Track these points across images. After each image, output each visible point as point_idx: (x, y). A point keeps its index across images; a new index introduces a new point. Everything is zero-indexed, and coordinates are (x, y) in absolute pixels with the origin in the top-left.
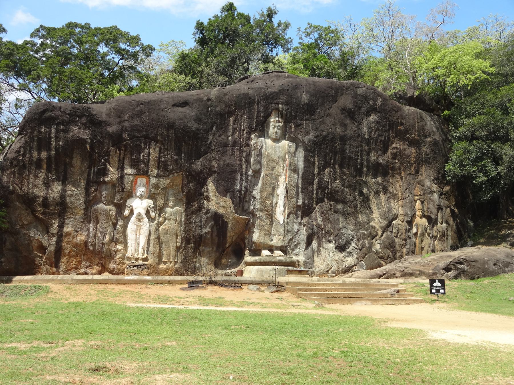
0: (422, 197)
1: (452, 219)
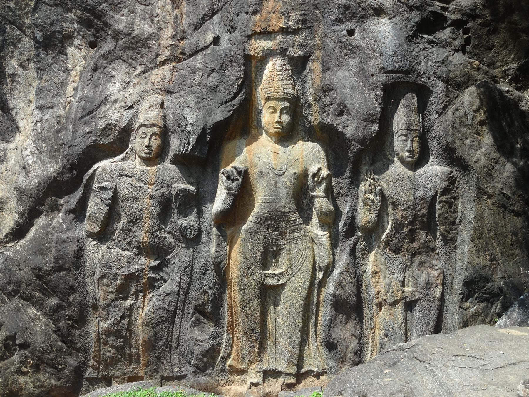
0: (299, 39)
1: (488, 140)
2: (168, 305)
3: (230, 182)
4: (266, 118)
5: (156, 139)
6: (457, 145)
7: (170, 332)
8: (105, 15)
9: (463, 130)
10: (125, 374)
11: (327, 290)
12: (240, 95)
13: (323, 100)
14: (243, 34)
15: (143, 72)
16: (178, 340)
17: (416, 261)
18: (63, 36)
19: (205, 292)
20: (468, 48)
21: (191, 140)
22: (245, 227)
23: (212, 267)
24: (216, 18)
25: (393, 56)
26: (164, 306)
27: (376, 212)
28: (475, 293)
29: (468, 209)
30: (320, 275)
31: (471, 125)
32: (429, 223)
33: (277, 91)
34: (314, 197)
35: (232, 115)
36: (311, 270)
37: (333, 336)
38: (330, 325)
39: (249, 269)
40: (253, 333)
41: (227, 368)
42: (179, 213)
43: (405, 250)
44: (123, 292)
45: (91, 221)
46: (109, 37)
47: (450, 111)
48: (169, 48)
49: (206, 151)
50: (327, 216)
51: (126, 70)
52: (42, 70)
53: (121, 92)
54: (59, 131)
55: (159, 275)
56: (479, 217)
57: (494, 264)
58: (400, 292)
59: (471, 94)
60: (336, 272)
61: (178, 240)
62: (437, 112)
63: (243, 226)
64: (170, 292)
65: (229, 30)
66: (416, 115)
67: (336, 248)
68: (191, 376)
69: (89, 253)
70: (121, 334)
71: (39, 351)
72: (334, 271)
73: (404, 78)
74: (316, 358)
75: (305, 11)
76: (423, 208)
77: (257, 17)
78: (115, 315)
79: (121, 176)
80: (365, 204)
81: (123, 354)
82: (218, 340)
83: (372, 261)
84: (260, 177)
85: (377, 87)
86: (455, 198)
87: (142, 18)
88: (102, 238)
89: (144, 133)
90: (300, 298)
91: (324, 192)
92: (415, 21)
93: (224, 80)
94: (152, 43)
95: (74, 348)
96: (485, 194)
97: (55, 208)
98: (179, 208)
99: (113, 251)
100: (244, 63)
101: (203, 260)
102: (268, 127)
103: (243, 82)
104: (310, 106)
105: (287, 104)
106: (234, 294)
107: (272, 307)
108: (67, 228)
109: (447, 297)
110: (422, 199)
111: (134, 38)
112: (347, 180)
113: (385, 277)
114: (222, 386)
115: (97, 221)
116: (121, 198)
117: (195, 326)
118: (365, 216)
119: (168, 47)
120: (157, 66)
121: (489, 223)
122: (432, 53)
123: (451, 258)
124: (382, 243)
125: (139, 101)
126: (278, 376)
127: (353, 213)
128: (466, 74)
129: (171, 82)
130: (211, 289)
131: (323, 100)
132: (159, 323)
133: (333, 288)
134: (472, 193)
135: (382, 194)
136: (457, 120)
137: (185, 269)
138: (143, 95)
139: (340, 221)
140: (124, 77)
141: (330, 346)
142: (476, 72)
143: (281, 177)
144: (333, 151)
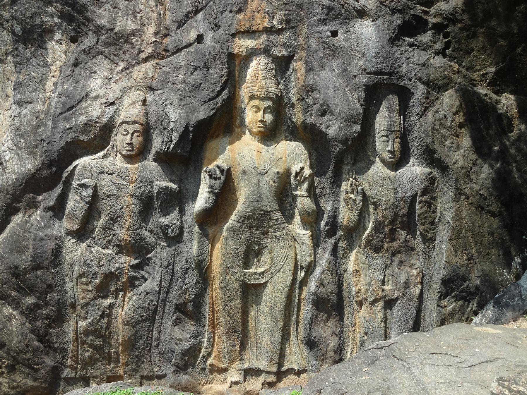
0: (283, 38)
1: (466, 142)
2: (149, 304)
3: (212, 180)
4: (250, 117)
5: (138, 136)
6: (437, 146)
7: (150, 331)
8: (87, 10)
9: (443, 131)
10: (104, 374)
11: (309, 288)
12: (223, 94)
13: (306, 100)
14: (227, 32)
15: (126, 69)
16: (158, 339)
17: (396, 260)
18: (43, 30)
19: (186, 291)
20: (448, 52)
21: (173, 138)
22: (227, 225)
23: (193, 266)
24: (200, 16)
25: (375, 57)
26: (144, 304)
27: (357, 212)
28: (452, 291)
29: (446, 209)
30: (301, 274)
31: (450, 127)
32: (408, 223)
33: (261, 90)
34: (296, 196)
35: (215, 113)
36: (293, 269)
37: (314, 335)
38: (311, 325)
39: (231, 268)
40: (234, 332)
41: (208, 367)
42: (161, 211)
43: (385, 249)
44: (102, 291)
45: (70, 219)
46: (91, 33)
47: (430, 113)
48: (152, 45)
49: (188, 149)
50: (309, 215)
51: (108, 66)
52: (21, 64)
53: (102, 89)
54: (38, 127)
55: (139, 273)
56: (457, 217)
57: (471, 263)
58: (380, 291)
59: (450, 97)
60: (318, 271)
61: (160, 238)
62: (418, 114)
63: (225, 224)
64: (151, 291)
65: (213, 29)
66: (397, 117)
67: (318, 247)
68: (172, 375)
69: (68, 251)
70: (101, 333)
71: (15, 351)
72: (316, 270)
73: (386, 80)
74: (296, 356)
75: (290, 11)
76: (404, 208)
77: (241, 16)
78: (94, 314)
79: (102, 173)
80: (347, 204)
81: (103, 354)
82: (199, 339)
83: (353, 260)
84: (243, 176)
85: (360, 88)
86: (434, 198)
87: (125, 14)
88: (82, 236)
89: (126, 130)
90: (282, 296)
91: (306, 191)
92: (397, 24)
93: (208, 78)
94: (135, 39)
95: (51, 347)
96: (463, 194)
97: (33, 205)
98: (160, 207)
99: (93, 249)
100: (228, 61)
101: (185, 258)
102: (251, 125)
103: (226, 81)
104: (293, 106)
105: (270, 103)
106: (216, 293)
107: (254, 306)
108: (45, 225)
109: (425, 296)
110: (402, 199)
111: (116, 33)
112: (330, 179)
113: (366, 276)
114: (203, 385)
115: (77, 218)
116: (101, 196)
117: (176, 325)
118: (346, 216)
119: (151, 43)
120: (139, 63)
121: (466, 223)
122: (414, 56)
123: (430, 257)
124: (363, 243)
125: (121, 98)
126: (259, 374)
127: (335, 212)
128: (446, 77)
129: (154, 79)
130: (193, 287)
131: (306, 100)
132: (139, 322)
133: (314, 287)
134: (451, 194)
135: (363, 193)
136: (437, 122)
137: (166, 268)
138: (125, 91)
139: (322, 220)
140: (106, 73)
141: (311, 344)
142: (456, 76)
143: (264, 176)
144: (316, 150)
